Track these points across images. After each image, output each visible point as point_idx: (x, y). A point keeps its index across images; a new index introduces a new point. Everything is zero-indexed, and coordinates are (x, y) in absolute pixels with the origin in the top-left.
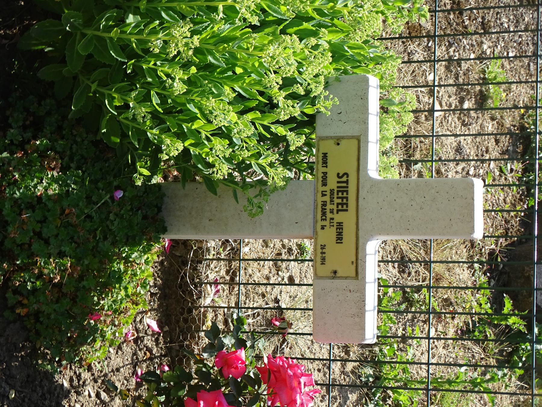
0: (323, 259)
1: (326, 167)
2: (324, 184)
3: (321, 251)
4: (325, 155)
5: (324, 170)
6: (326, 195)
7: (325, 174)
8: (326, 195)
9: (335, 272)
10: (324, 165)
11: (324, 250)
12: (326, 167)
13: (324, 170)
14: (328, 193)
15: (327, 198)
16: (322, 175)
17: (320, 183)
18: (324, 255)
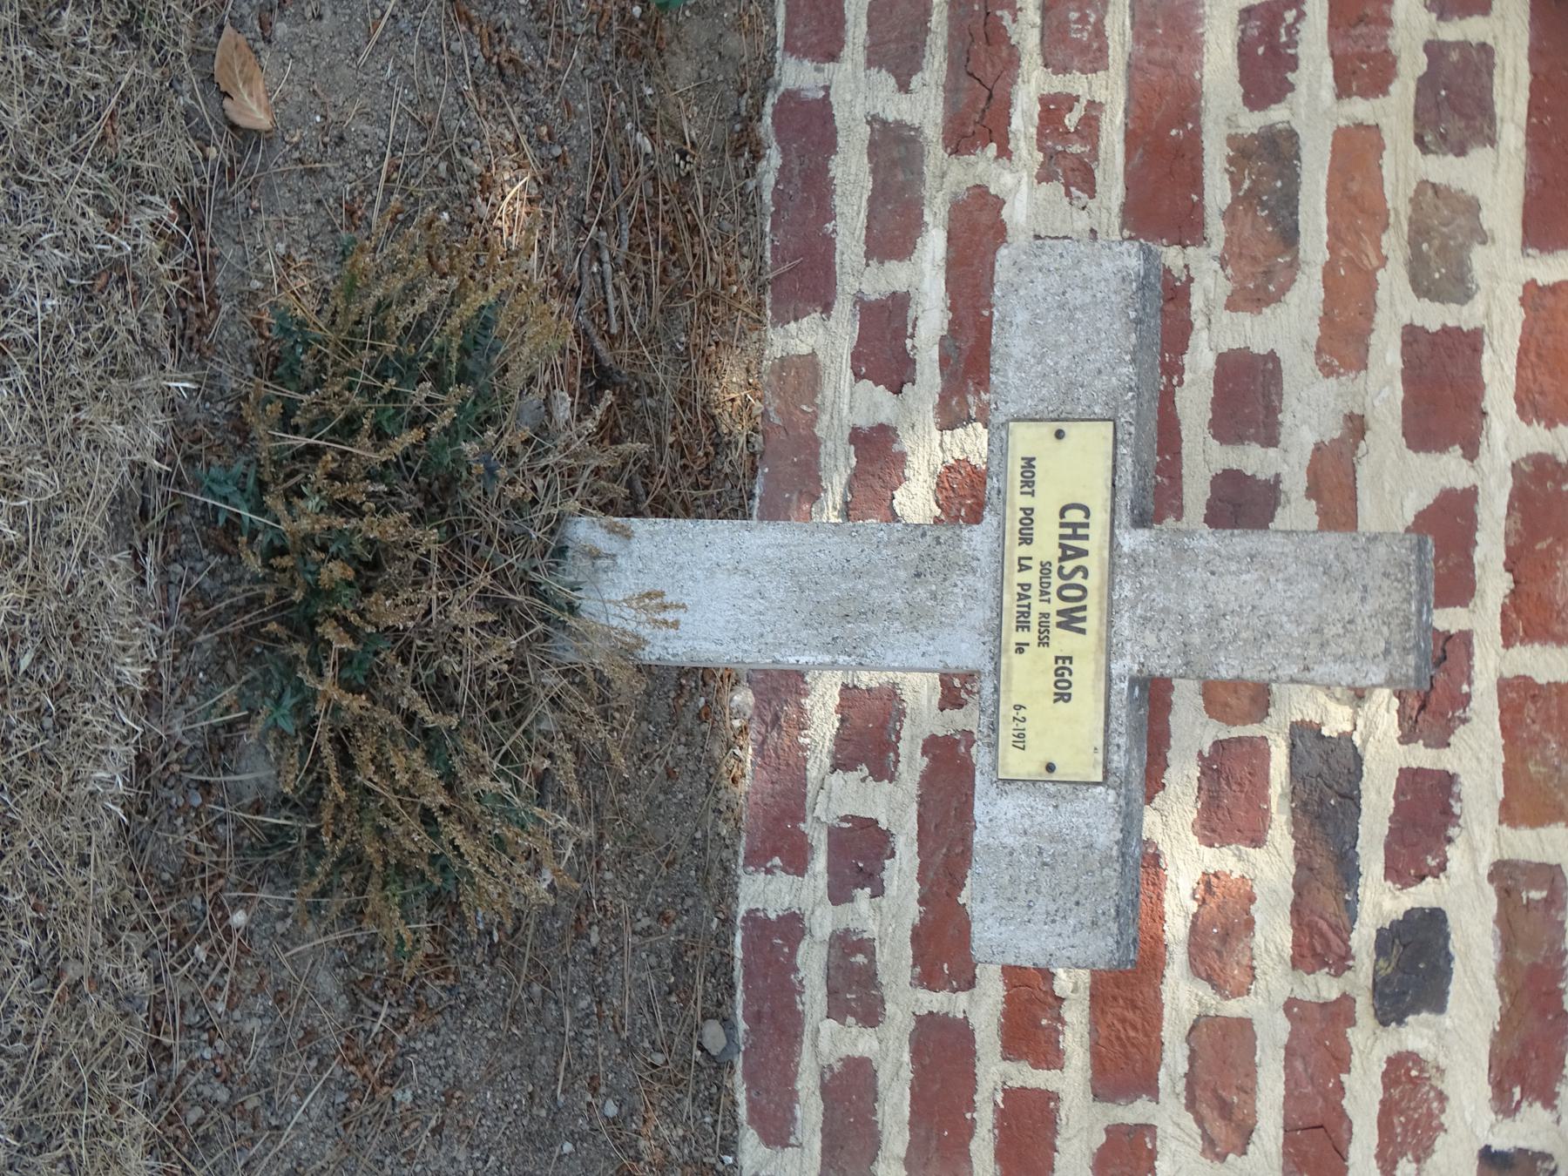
0: (1021, 736)
1: (1032, 494)
2: (1026, 539)
3: (1014, 713)
4: (1029, 463)
5: (1026, 501)
6: (1029, 568)
7: (1028, 512)
8: (1029, 568)
9: (1050, 768)
10: (1026, 489)
11: (1022, 713)
12: (1032, 494)
13: (1026, 501)
14: (1036, 568)
15: (1032, 577)
16: (1021, 514)
17: (1012, 537)
18: (1021, 725)
